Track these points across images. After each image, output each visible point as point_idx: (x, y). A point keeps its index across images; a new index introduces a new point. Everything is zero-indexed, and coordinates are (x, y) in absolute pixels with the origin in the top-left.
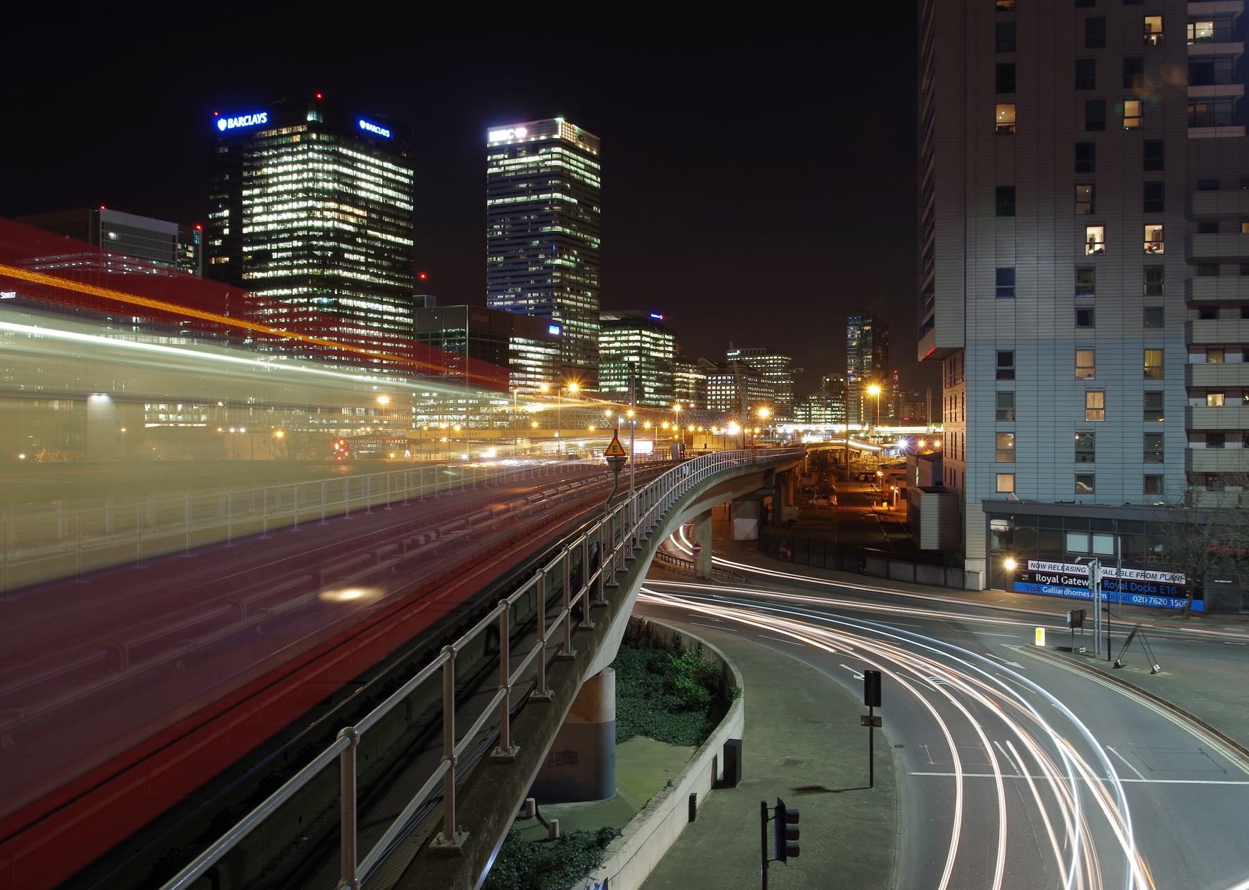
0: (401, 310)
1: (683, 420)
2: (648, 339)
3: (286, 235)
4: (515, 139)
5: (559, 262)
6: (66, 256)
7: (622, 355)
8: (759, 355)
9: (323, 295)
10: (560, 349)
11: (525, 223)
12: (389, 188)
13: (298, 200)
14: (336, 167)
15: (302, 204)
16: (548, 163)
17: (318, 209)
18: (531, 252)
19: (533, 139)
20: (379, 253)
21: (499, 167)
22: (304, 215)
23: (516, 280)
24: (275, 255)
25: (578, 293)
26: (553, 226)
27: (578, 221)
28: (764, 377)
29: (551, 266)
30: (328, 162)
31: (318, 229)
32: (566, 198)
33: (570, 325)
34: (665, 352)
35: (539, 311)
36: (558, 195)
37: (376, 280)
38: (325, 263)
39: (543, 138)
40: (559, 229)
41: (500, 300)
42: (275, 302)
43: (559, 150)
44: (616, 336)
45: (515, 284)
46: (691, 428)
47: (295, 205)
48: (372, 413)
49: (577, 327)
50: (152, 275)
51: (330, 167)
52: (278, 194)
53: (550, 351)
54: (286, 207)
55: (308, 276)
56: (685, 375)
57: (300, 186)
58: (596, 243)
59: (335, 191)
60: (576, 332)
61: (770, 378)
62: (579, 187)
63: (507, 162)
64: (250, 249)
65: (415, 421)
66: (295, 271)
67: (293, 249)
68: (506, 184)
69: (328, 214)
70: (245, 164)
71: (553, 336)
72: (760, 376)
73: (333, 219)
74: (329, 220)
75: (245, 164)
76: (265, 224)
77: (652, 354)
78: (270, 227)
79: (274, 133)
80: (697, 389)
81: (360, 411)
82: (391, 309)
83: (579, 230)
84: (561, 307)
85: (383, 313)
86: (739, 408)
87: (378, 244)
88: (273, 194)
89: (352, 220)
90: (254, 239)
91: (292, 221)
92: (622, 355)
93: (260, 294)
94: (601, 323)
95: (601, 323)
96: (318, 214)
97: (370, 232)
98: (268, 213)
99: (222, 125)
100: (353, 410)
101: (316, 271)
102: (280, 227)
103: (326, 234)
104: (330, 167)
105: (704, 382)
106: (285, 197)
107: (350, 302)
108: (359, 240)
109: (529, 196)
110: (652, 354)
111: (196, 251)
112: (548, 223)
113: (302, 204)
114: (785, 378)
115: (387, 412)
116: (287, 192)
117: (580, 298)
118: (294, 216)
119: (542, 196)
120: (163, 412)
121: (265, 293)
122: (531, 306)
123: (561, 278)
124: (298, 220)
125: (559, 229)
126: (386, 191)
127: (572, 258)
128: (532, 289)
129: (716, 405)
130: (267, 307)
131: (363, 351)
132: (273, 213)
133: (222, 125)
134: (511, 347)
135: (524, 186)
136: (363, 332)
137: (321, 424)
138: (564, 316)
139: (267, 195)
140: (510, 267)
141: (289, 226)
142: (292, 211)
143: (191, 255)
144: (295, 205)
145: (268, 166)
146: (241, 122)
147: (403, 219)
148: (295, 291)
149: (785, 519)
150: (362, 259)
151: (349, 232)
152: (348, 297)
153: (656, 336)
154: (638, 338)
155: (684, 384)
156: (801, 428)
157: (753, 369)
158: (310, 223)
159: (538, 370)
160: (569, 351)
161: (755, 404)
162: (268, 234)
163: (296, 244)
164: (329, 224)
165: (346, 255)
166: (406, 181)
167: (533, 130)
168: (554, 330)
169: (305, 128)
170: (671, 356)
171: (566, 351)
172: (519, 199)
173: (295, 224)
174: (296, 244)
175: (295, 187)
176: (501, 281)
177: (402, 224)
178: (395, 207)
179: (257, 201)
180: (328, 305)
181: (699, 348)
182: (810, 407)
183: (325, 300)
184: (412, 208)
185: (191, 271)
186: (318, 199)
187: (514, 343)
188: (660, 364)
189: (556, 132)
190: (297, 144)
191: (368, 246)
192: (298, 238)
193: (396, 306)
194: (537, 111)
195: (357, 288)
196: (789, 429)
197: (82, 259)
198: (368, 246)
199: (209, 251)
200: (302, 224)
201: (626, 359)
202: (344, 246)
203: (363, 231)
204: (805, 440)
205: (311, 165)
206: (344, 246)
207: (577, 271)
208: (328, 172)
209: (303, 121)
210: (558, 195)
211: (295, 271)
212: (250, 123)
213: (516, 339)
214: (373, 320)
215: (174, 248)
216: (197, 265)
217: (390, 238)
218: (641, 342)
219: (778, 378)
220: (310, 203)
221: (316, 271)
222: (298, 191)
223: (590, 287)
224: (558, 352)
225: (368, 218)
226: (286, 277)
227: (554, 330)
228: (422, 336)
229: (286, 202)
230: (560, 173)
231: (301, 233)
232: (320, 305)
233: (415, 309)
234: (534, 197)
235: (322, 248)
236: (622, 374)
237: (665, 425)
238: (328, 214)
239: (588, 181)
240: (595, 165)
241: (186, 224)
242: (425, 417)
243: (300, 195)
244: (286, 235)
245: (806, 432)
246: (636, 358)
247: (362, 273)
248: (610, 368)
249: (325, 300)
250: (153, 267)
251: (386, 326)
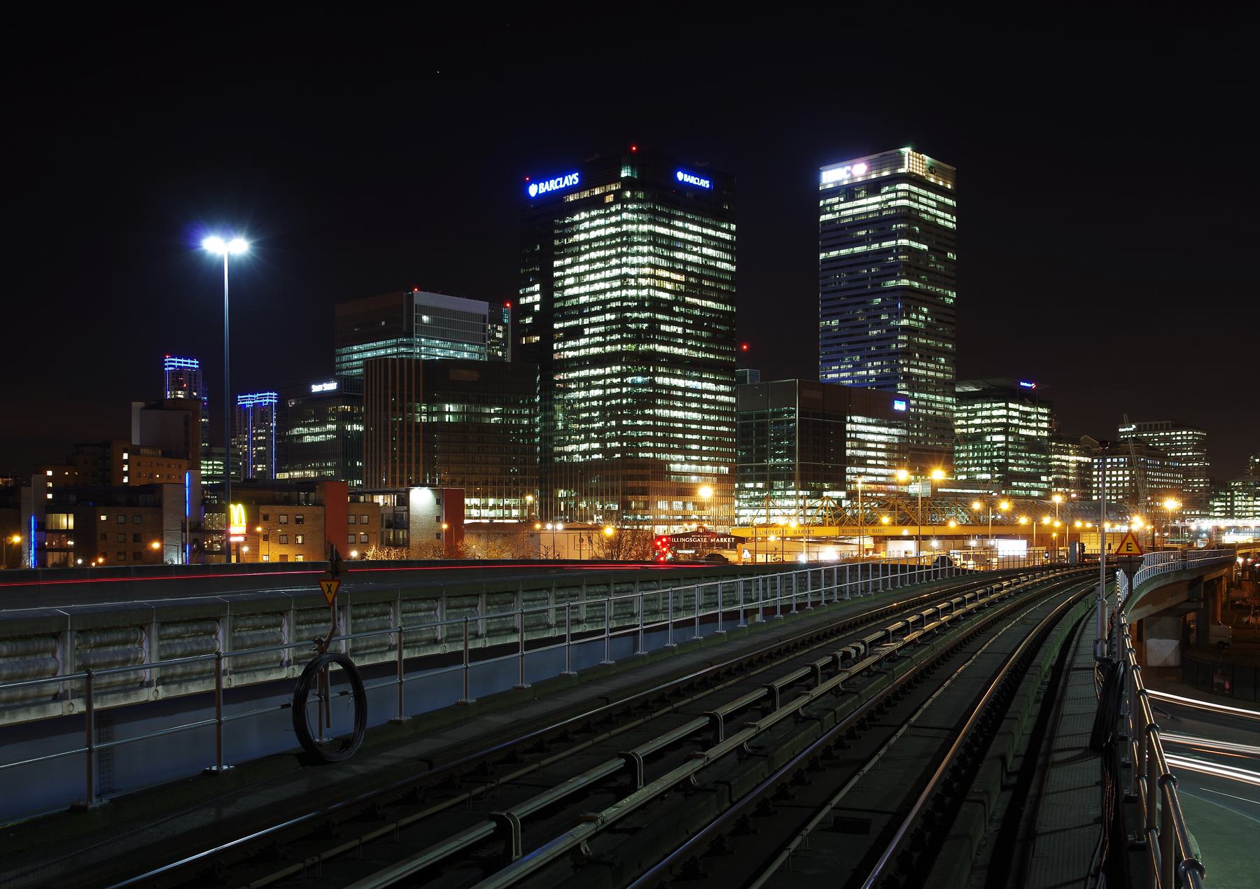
0: (722, 388)
1: (1068, 512)
2: (1017, 414)
3: (598, 308)
4: (852, 178)
5: (905, 322)
6: (381, 343)
7: (984, 434)
8: (1162, 430)
9: (637, 374)
10: (907, 428)
11: (865, 278)
12: (708, 247)
13: (611, 268)
14: (651, 227)
15: (616, 272)
16: (892, 204)
17: (632, 277)
18: (873, 312)
19: (874, 176)
20: (698, 323)
21: (833, 212)
22: (617, 284)
23: (853, 347)
24: (587, 331)
25: (929, 360)
26: (898, 279)
27: (928, 271)
28: (1169, 459)
29: (896, 328)
30: (643, 222)
31: (633, 299)
32: (914, 245)
33: (918, 400)
34: (1038, 429)
35: (881, 383)
36: (905, 242)
37: (695, 354)
38: (639, 337)
39: (886, 173)
40: (905, 282)
41: (835, 372)
42: (588, 383)
43: (905, 186)
44: (975, 411)
45: (853, 352)
46: (1078, 524)
47: (608, 274)
48: (690, 507)
49: (927, 401)
50: (463, 360)
51: (644, 228)
52: (591, 262)
53: (894, 431)
54: (598, 276)
55: (621, 353)
56: (1063, 457)
57: (613, 252)
58: (951, 297)
59: (650, 254)
60: (927, 408)
61: (1177, 459)
62: (930, 230)
63: (842, 206)
64: (561, 325)
65: (737, 516)
66: (608, 348)
67: (606, 323)
68: (842, 233)
69: (643, 282)
70: (557, 232)
71: (899, 412)
72: (1163, 457)
73: (649, 287)
74: (644, 288)
75: (557, 232)
76: (577, 296)
77: (1022, 432)
78: (583, 300)
79: (586, 194)
80: (1079, 474)
81: (677, 505)
82: (711, 386)
83: (931, 282)
84: (908, 377)
85: (702, 391)
86: (1133, 498)
87: (697, 312)
88: (585, 262)
89: (669, 286)
91: (604, 291)
92: (984, 434)
93: (571, 375)
94: (958, 395)
95: (958, 395)
96: (632, 282)
97: (688, 299)
98: (580, 284)
99: (533, 190)
100: (670, 504)
101: (630, 347)
102: (593, 299)
103: (641, 304)
104: (644, 228)
105: (1089, 466)
106: (599, 265)
107: (667, 381)
108: (676, 309)
109: (869, 244)
110: (1022, 432)
111: (505, 331)
112: (893, 276)
113: (616, 272)
114: (1198, 459)
115: (709, 505)
116: (600, 259)
117: (931, 366)
118: (607, 285)
119: (885, 245)
120: (476, 507)
121: (576, 374)
122: (872, 377)
123: (909, 342)
124: (612, 290)
125: (905, 282)
126: (705, 251)
127: (922, 317)
128: (873, 357)
129: (1104, 495)
130: (579, 389)
131: (680, 436)
132: (585, 284)
133: (533, 190)
134: (848, 427)
135: (863, 233)
136: (680, 414)
137: (635, 519)
138: (912, 388)
139: (580, 264)
140: (847, 331)
141: (602, 297)
142: (605, 280)
143: (500, 335)
144: (608, 274)
145: (579, 232)
146: (552, 185)
147: (724, 282)
148: (608, 370)
149: (1213, 640)
150: (680, 330)
151: (665, 301)
152: (664, 375)
153: (1027, 409)
154: (1004, 412)
155: (1062, 469)
156: (1223, 523)
157: (1154, 448)
158: (624, 293)
159: (880, 454)
160: (918, 430)
161: (1158, 493)
162: (581, 307)
163: (609, 317)
164: (644, 293)
165: (663, 327)
166: (728, 237)
167: (873, 166)
168: (900, 406)
169: (619, 187)
170: (1046, 434)
171: (914, 430)
172: (858, 249)
173: (608, 295)
174: (609, 317)
175: (608, 253)
176: (835, 348)
177: (724, 287)
178: (715, 269)
179: (568, 271)
180: (643, 385)
181: (1083, 424)
182: (1232, 496)
183: (640, 379)
184: (733, 268)
185: (500, 354)
186: (633, 266)
187: (852, 422)
188: (1033, 445)
189: (902, 165)
190: (611, 204)
191: (686, 316)
192: (612, 311)
193: (717, 383)
194: (878, 144)
195: (674, 363)
196: (1206, 525)
197: (397, 346)
198: (686, 316)
199: (518, 330)
200: (616, 294)
201: (988, 439)
202: (660, 317)
203: (680, 298)
204: (1228, 539)
205: (625, 228)
206: (660, 317)
207: (929, 331)
208: (643, 234)
209: (616, 178)
210: (905, 242)
211: (608, 348)
212: (562, 186)
213: (855, 418)
214: (692, 400)
215: (484, 329)
216: (506, 346)
217: (710, 304)
218: (1008, 417)
219: (1188, 459)
220: (625, 270)
221: (630, 347)
222: (610, 257)
223: (944, 352)
224: (904, 432)
225: (686, 283)
226: (599, 355)
227: (900, 406)
228: (744, 417)
229: (599, 270)
230: (907, 215)
231: (614, 305)
232: (634, 385)
233: (738, 386)
234: (876, 246)
235: (637, 320)
236: (983, 458)
237: (1046, 520)
238: (643, 282)
239: (941, 222)
240: (950, 202)
241: (496, 304)
242: (750, 512)
243: (614, 262)
244: (598, 308)
245: (1229, 529)
246: (1002, 438)
247: (680, 346)
248: (968, 451)
249: (640, 379)
250: (464, 350)
251: (705, 406)
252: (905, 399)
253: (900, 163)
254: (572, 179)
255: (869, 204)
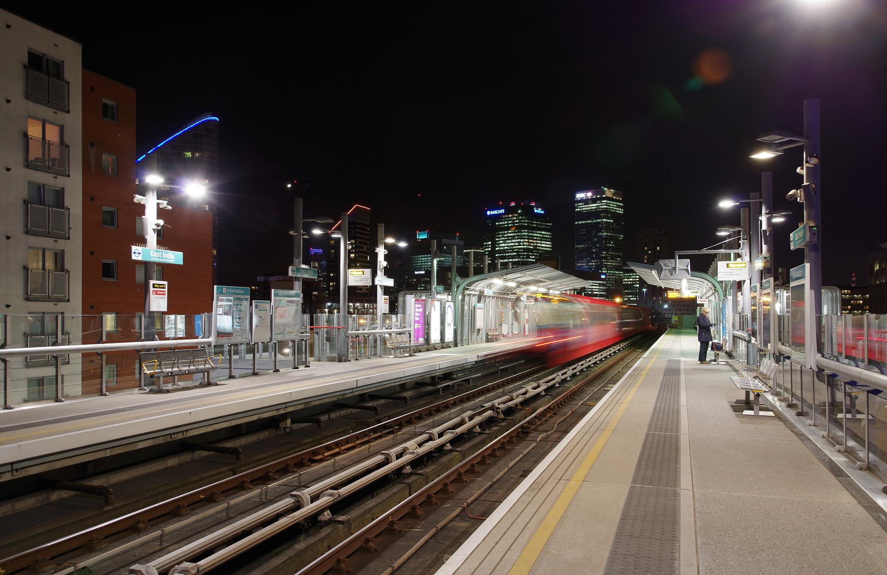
62: (614, 215)
84: (606, 265)
90: (499, 252)
128: (594, 259)
168: (603, 277)
223: (619, 256)
227: (603, 277)
230: (606, 211)
252: (604, 274)
253: (604, 193)
254: (502, 211)
255: (593, 206)
